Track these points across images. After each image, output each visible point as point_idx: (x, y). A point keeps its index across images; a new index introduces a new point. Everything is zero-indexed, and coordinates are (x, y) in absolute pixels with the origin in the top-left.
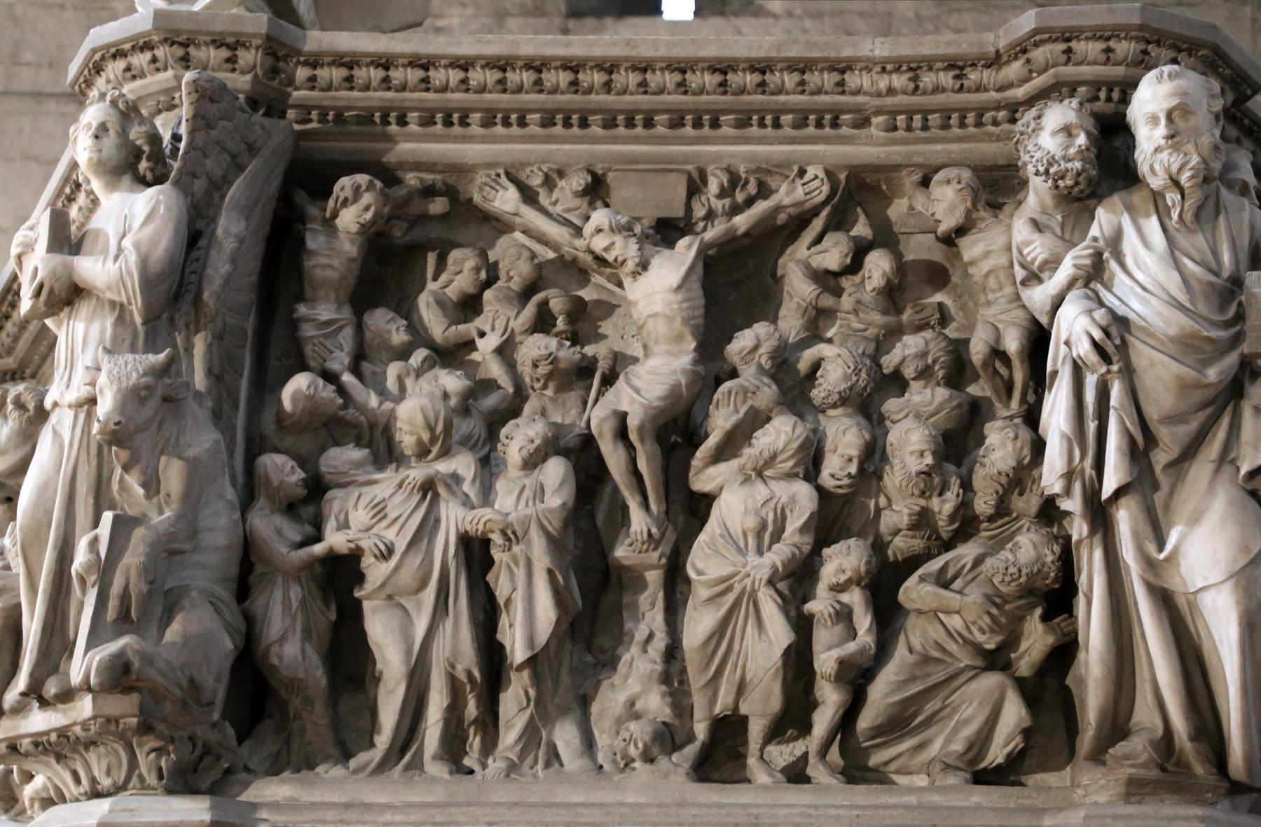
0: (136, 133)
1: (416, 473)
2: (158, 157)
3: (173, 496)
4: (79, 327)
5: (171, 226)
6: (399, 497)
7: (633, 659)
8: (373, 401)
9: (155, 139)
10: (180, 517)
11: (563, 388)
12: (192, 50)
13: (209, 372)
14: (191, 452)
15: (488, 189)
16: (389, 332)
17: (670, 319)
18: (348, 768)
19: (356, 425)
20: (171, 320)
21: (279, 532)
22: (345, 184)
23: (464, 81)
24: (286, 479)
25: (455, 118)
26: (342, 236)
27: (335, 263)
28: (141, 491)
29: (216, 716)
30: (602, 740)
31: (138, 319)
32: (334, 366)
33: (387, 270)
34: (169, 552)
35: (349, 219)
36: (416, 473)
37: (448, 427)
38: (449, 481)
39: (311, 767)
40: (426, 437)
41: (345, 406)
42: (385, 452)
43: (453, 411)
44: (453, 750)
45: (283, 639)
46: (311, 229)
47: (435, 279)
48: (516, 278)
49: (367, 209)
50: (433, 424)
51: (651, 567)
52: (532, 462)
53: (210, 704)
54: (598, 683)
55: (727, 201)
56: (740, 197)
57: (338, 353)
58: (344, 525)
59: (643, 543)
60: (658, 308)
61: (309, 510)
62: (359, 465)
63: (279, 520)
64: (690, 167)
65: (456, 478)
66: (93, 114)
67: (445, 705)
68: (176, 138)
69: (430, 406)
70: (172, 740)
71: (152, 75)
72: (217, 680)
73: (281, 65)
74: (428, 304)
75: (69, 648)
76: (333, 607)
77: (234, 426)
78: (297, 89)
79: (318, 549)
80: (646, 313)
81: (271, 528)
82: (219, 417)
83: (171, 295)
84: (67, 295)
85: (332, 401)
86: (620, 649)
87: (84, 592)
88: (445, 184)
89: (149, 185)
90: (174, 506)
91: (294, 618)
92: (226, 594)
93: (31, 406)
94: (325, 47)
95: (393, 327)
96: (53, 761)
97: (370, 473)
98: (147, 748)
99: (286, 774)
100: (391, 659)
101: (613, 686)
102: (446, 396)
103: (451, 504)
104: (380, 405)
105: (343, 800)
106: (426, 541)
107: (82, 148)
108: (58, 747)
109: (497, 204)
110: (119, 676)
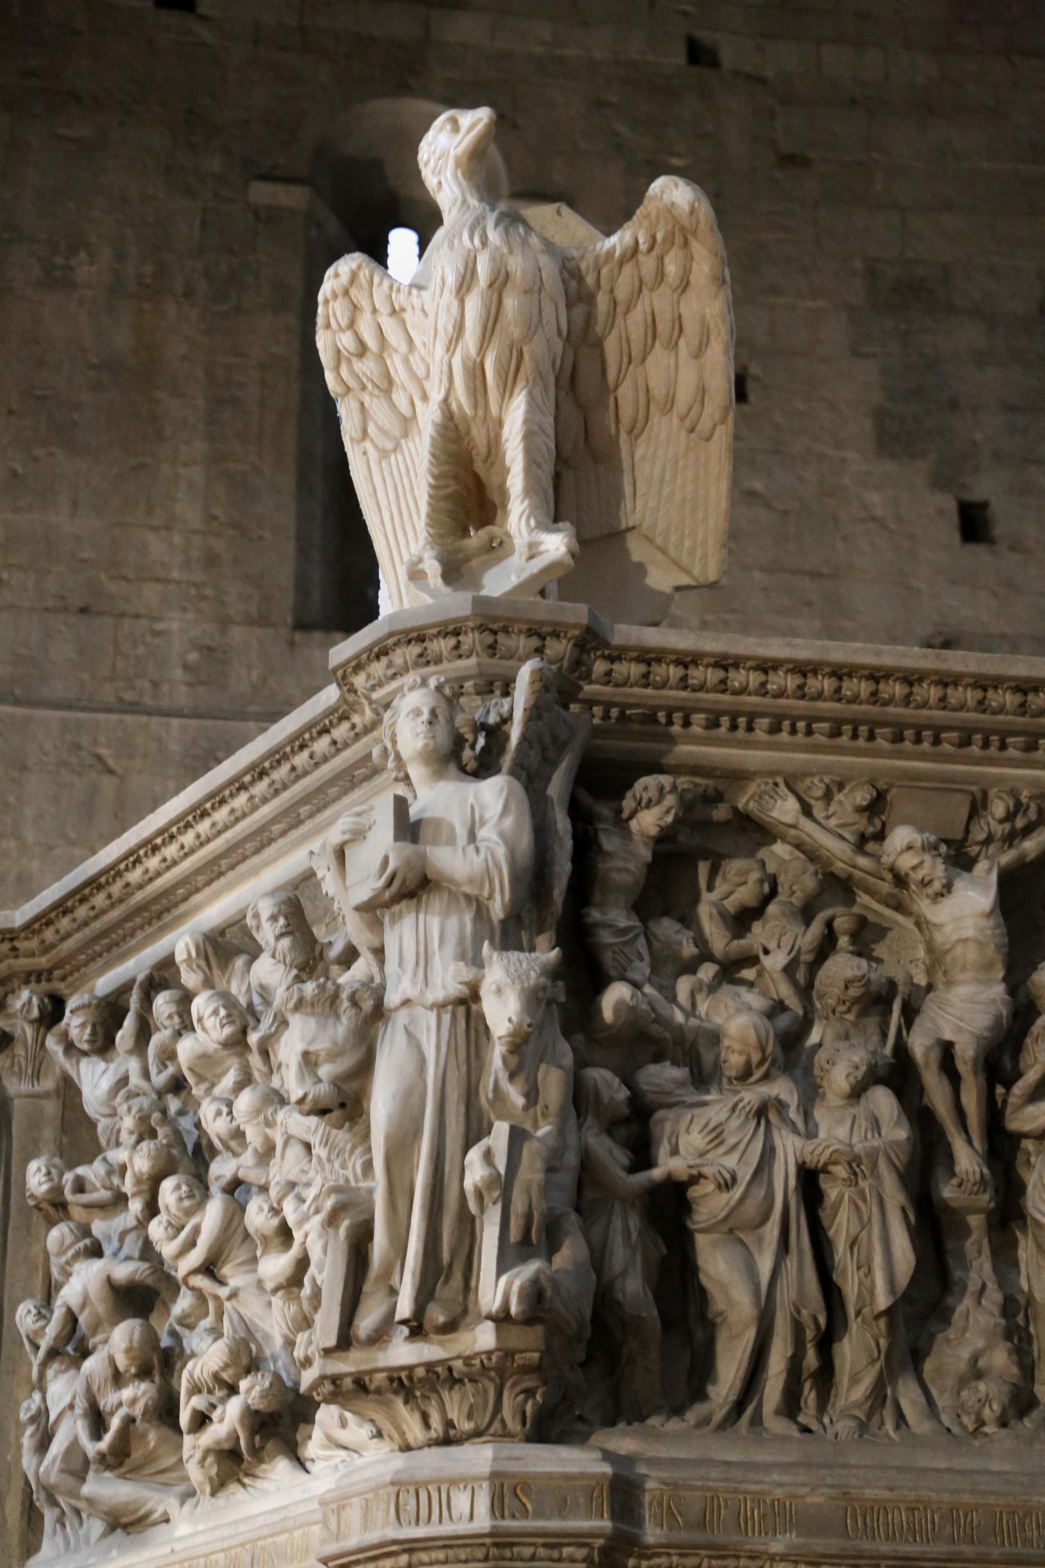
6: (735, 1123)
7: (968, 1310)
11: (863, 1013)
15: (767, 798)
16: (680, 944)
17: (981, 945)
23: (684, 678)
25: (739, 721)
26: (637, 838)
27: (632, 866)
30: (942, 1401)
36: (750, 1096)
39: (642, 1419)
40: (756, 1057)
44: (791, 1406)
45: (624, 1274)
46: (605, 830)
47: (710, 888)
48: (798, 894)
49: (668, 812)
51: (976, 1211)
52: (857, 1093)
54: (932, 1337)
55: (1007, 826)
56: (1020, 823)
57: (637, 963)
59: (974, 1184)
60: (970, 933)
62: (682, 1084)
64: (974, 788)
65: (781, 1106)
67: (789, 1354)
71: (449, 661)
73: (585, 657)
74: (711, 916)
78: (591, 683)
80: (955, 937)
86: (950, 1300)
88: (716, 789)
94: (633, 642)
99: (622, 1425)
101: (948, 1340)
109: (775, 814)
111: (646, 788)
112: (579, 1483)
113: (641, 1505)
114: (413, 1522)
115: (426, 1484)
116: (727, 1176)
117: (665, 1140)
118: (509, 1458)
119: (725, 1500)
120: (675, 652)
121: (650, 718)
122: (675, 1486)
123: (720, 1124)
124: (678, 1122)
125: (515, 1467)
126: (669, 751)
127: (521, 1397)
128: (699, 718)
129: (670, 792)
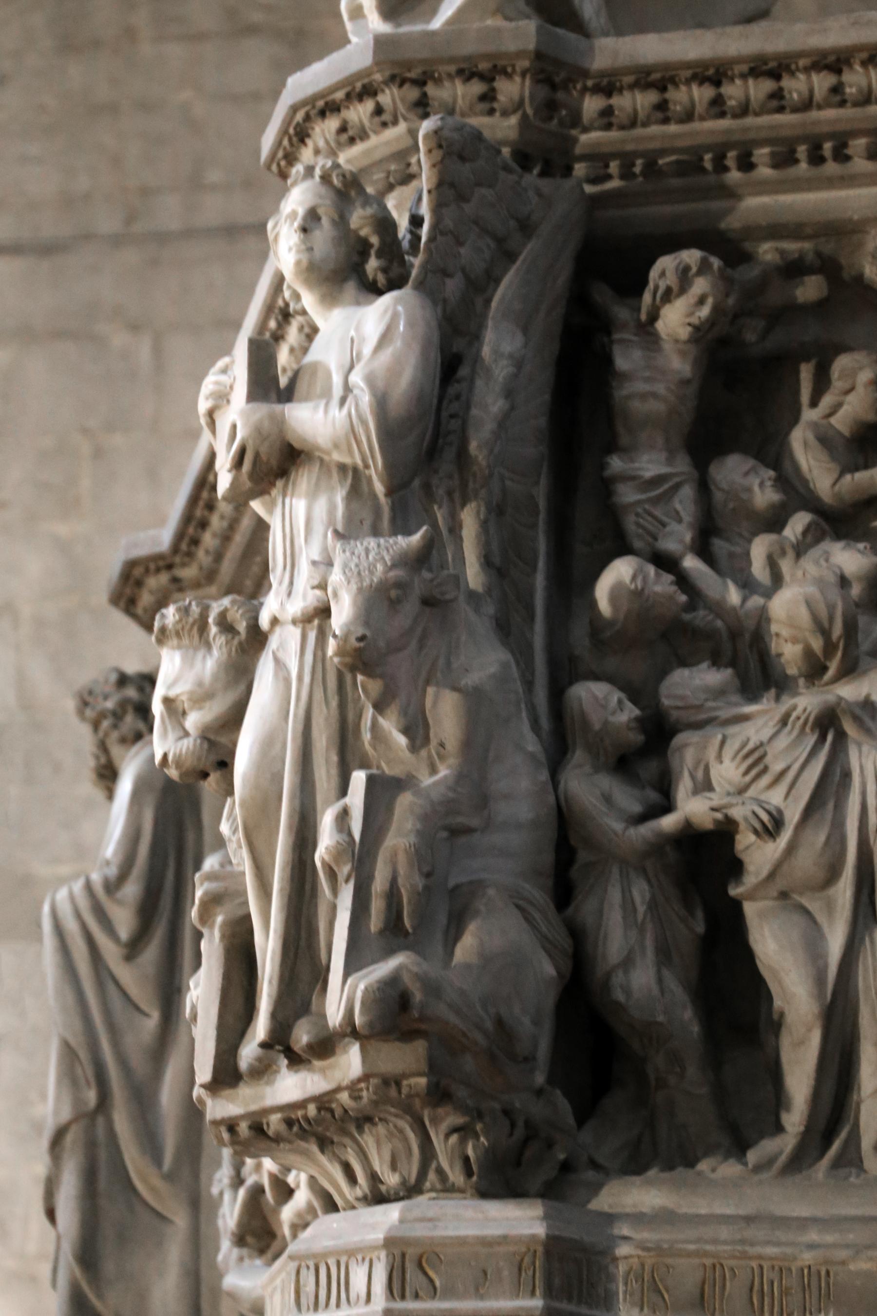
0: (359, 219)
1: (807, 702)
2: (391, 249)
3: (449, 746)
4: (299, 505)
5: (416, 348)
6: (783, 741)
8: (734, 596)
9: (385, 225)
10: (460, 777)
12: (431, 90)
13: (487, 562)
14: (471, 679)
16: (749, 490)
18: (745, 1164)
19: (710, 635)
20: (427, 488)
21: (607, 799)
22: (665, 267)
24: (612, 719)
28: (402, 740)
29: (540, 1079)
31: (379, 488)
32: (669, 545)
33: (740, 396)
34: (451, 829)
35: (675, 320)
37: (851, 628)
38: (858, 712)
40: (817, 644)
41: (691, 607)
42: (756, 671)
43: (857, 605)
45: (627, 963)
46: (622, 341)
50: (826, 624)
53: (529, 1059)
57: (674, 526)
58: (705, 786)
61: (649, 769)
62: (719, 693)
63: (606, 782)
66: (298, 198)
68: (416, 221)
69: (818, 596)
70: (480, 1116)
72: (536, 1023)
74: (806, 444)
75: (321, 976)
76: (700, 914)
77: (530, 646)
79: (668, 822)
81: (591, 789)
82: (504, 628)
83: (424, 449)
84: (278, 462)
85: (671, 598)
87: (335, 891)
88: (819, 254)
89: (380, 293)
90: (452, 761)
91: (642, 930)
92: (539, 895)
93: (242, 627)
95: (754, 482)
96: (314, 1148)
97: (736, 705)
98: (444, 1127)
100: (793, 988)
102: (844, 582)
103: (865, 748)
104: (744, 600)
105: (742, 1212)
106: (831, 805)
107: (286, 250)
108: (318, 1126)
110: (394, 1015)
111: (663, 274)
112: (501, 1249)
113: (611, 1278)
114: (312, 1307)
115: (325, 1255)
116: (765, 817)
117: (686, 774)
118: (423, 1220)
119: (732, 1269)
120: (687, 65)
121: (690, 166)
122: (658, 1250)
123: (762, 744)
124: (705, 747)
125: (420, 1231)
126: (730, 211)
127: (454, 1139)
128: (762, 153)
129: (700, 273)
